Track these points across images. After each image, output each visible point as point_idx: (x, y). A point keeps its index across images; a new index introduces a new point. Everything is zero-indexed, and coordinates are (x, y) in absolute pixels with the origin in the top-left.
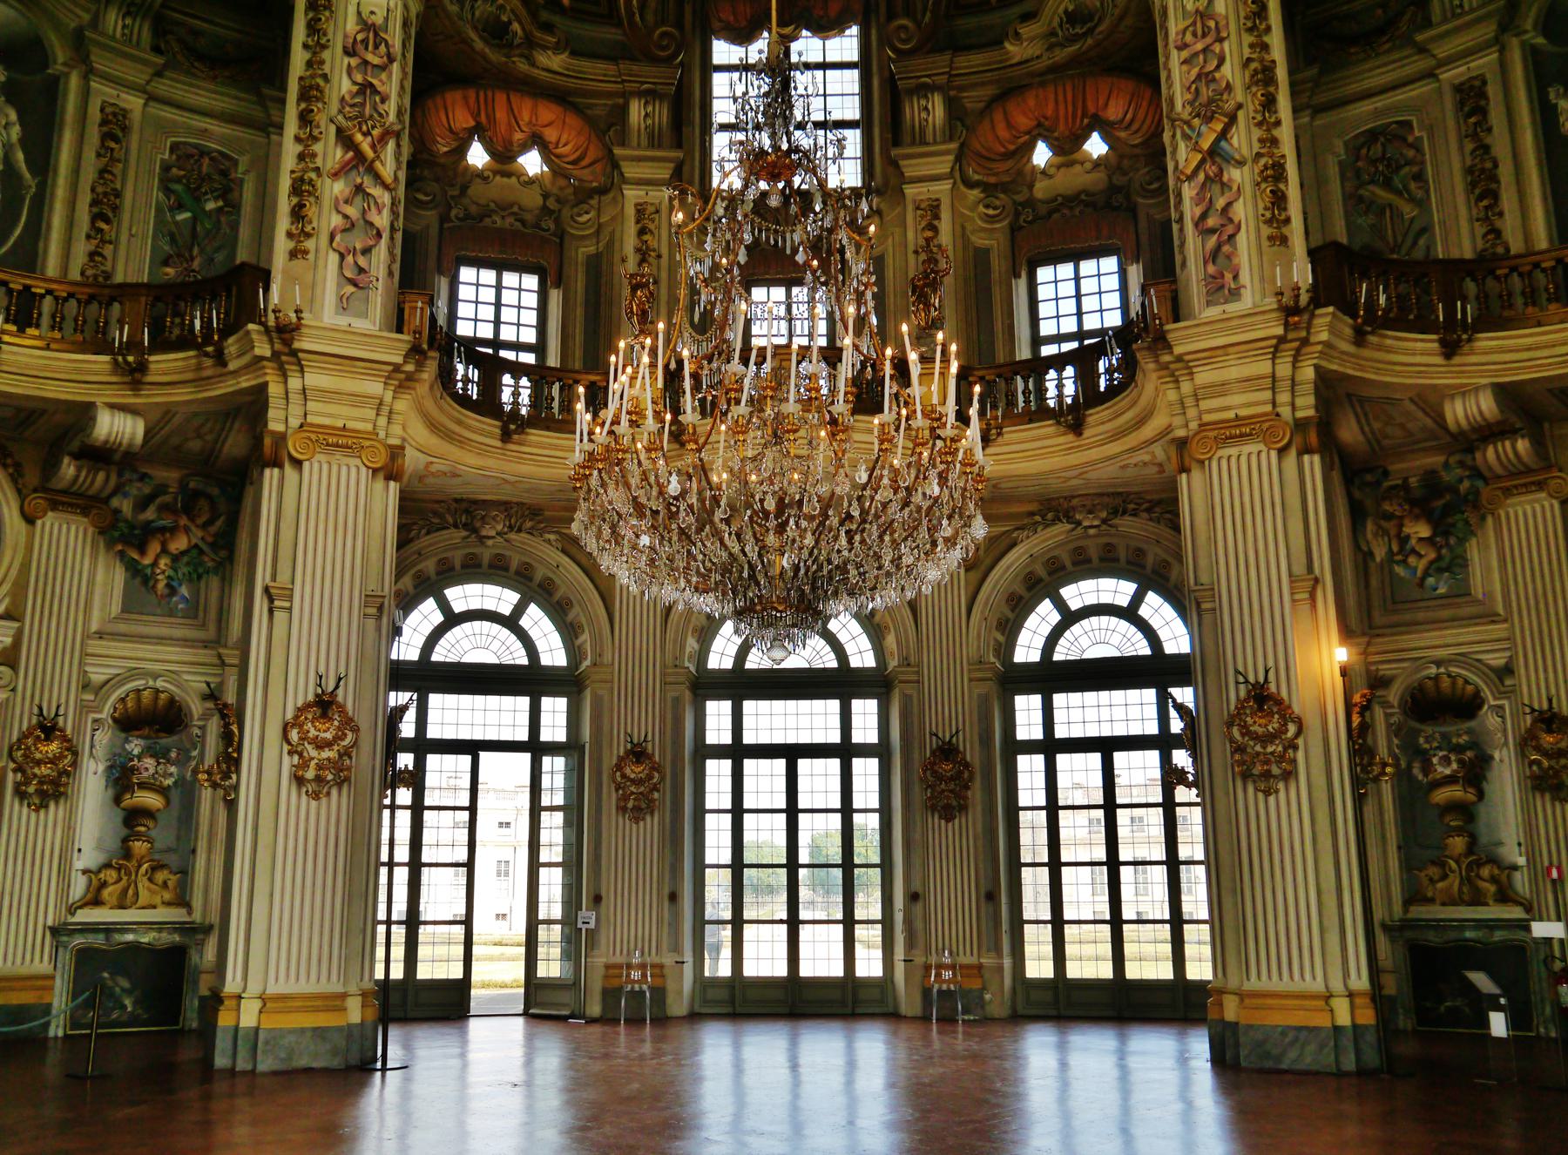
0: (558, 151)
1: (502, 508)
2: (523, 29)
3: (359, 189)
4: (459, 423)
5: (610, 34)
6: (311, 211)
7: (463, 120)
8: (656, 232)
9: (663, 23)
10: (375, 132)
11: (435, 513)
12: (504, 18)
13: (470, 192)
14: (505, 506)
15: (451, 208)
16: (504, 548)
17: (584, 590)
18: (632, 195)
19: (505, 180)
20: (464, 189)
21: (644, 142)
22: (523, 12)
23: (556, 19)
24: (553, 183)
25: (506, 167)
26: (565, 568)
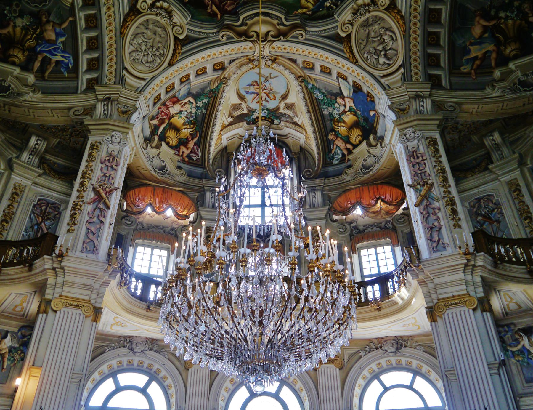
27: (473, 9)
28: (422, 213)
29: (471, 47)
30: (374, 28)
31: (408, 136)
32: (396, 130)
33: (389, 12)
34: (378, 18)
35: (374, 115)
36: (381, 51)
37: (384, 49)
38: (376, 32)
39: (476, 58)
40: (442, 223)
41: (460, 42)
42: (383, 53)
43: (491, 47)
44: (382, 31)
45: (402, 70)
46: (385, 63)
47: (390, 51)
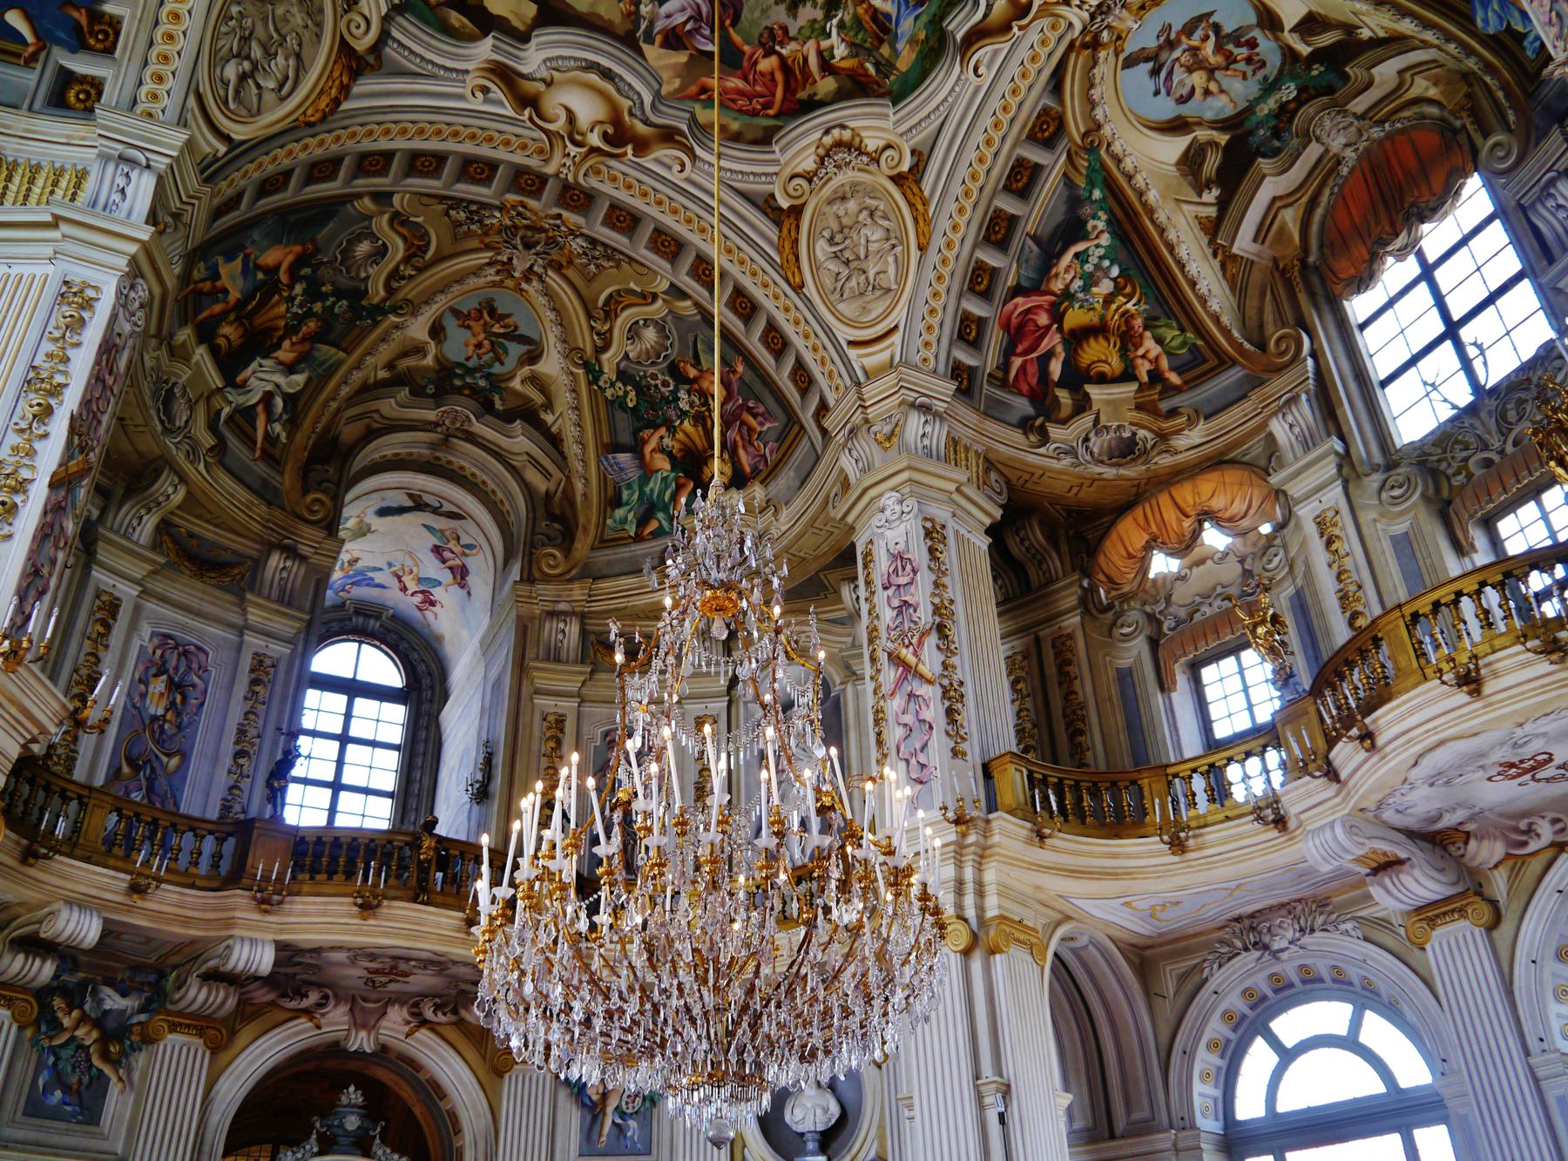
0: (1227, 515)
1: (1284, 912)
2: (1151, 430)
3: (911, 695)
4: (1114, 856)
5: (1232, 376)
6: (884, 736)
7: (1137, 539)
8: (1342, 535)
9: (1284, 325)
10: (914, 641)
11: (1223, 942)
12: (1127, 434)
13: (1174, 598)
14: (1285, 907)
15: (1159, 623)
16: (1301, 957)
17: (1401, 979)
18: (1306, 513)
19: (1202, 568)
20: (1168, 599)
21: (1299, 449)
22: (1143, 417)
23: (1176, 401)
24: (1245, 545)
25: (1197, 553)
26: (1374, 959)
27: (319, 237)
28: (45, 513)
29: (239, 260)
30: (295, 10)
31: (132, 294)
32: (133, 248)
33: (339, 57)
34: (319, 19)
35: (17, 37)
36: (248, 57)
37: (255, 65)
38: (287, 21)
39: (216, 276)
40: (53, 582)
41: (256, 235)
42: (247, 65)
43: (234, 295)
44: (291, 41)
45: (223, 149)
46: (226, 84)
47: (255, 91)
